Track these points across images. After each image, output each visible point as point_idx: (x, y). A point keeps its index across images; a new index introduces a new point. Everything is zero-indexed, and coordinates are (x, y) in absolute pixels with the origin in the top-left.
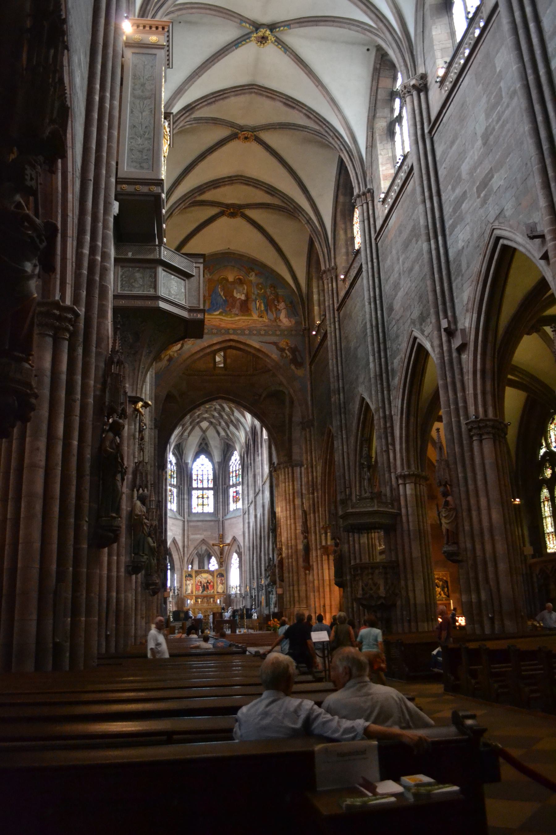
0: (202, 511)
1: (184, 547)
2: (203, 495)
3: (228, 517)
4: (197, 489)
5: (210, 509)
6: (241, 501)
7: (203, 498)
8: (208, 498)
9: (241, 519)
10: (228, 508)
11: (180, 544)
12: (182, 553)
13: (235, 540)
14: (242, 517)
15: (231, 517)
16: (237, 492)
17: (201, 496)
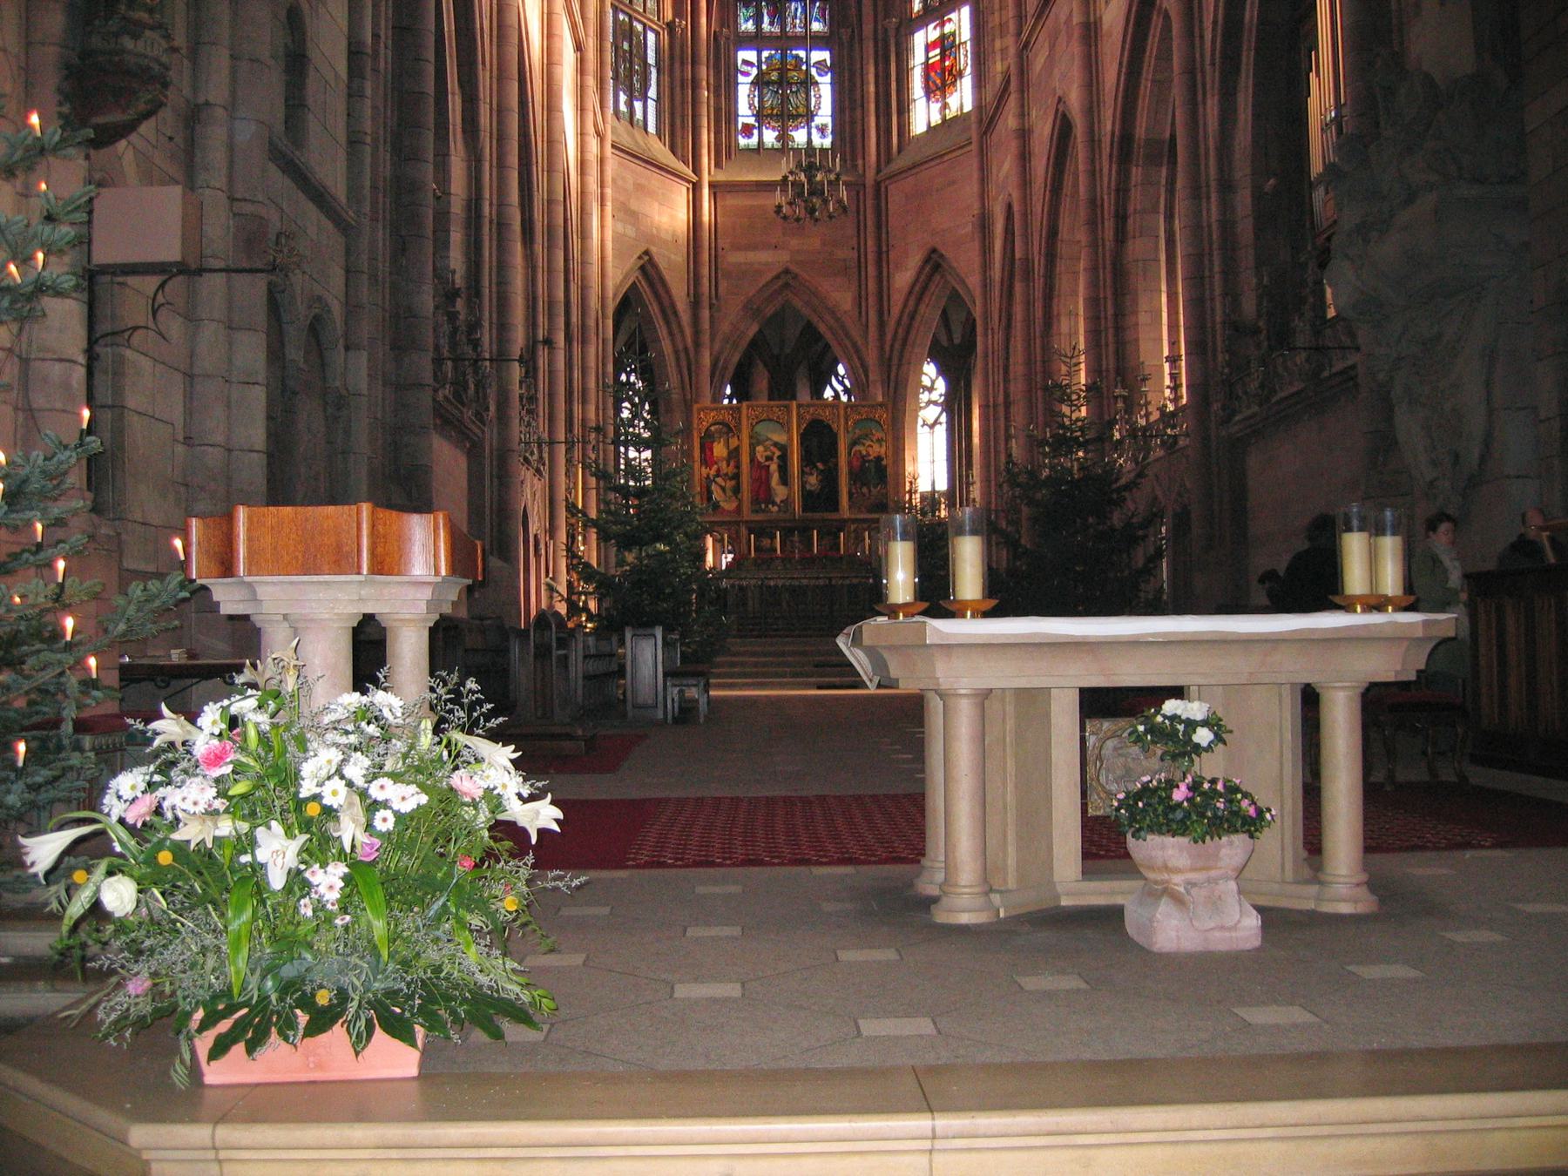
0: (778, 145)
1: (695, 305)
2: (783, 70)
3: (900, 163)
4: (757, 40)
5: (817, 132)
6: (966, 83)
7: (783, 82)
8: (808, 83)
9: (969, 167)
10: (904, 126)
11: (679, 291)
12: (688, 331)
13: (937, 267)
14: (974, 147)
15: (918, 159)
16: (946, 45)
17: (774, 76)
